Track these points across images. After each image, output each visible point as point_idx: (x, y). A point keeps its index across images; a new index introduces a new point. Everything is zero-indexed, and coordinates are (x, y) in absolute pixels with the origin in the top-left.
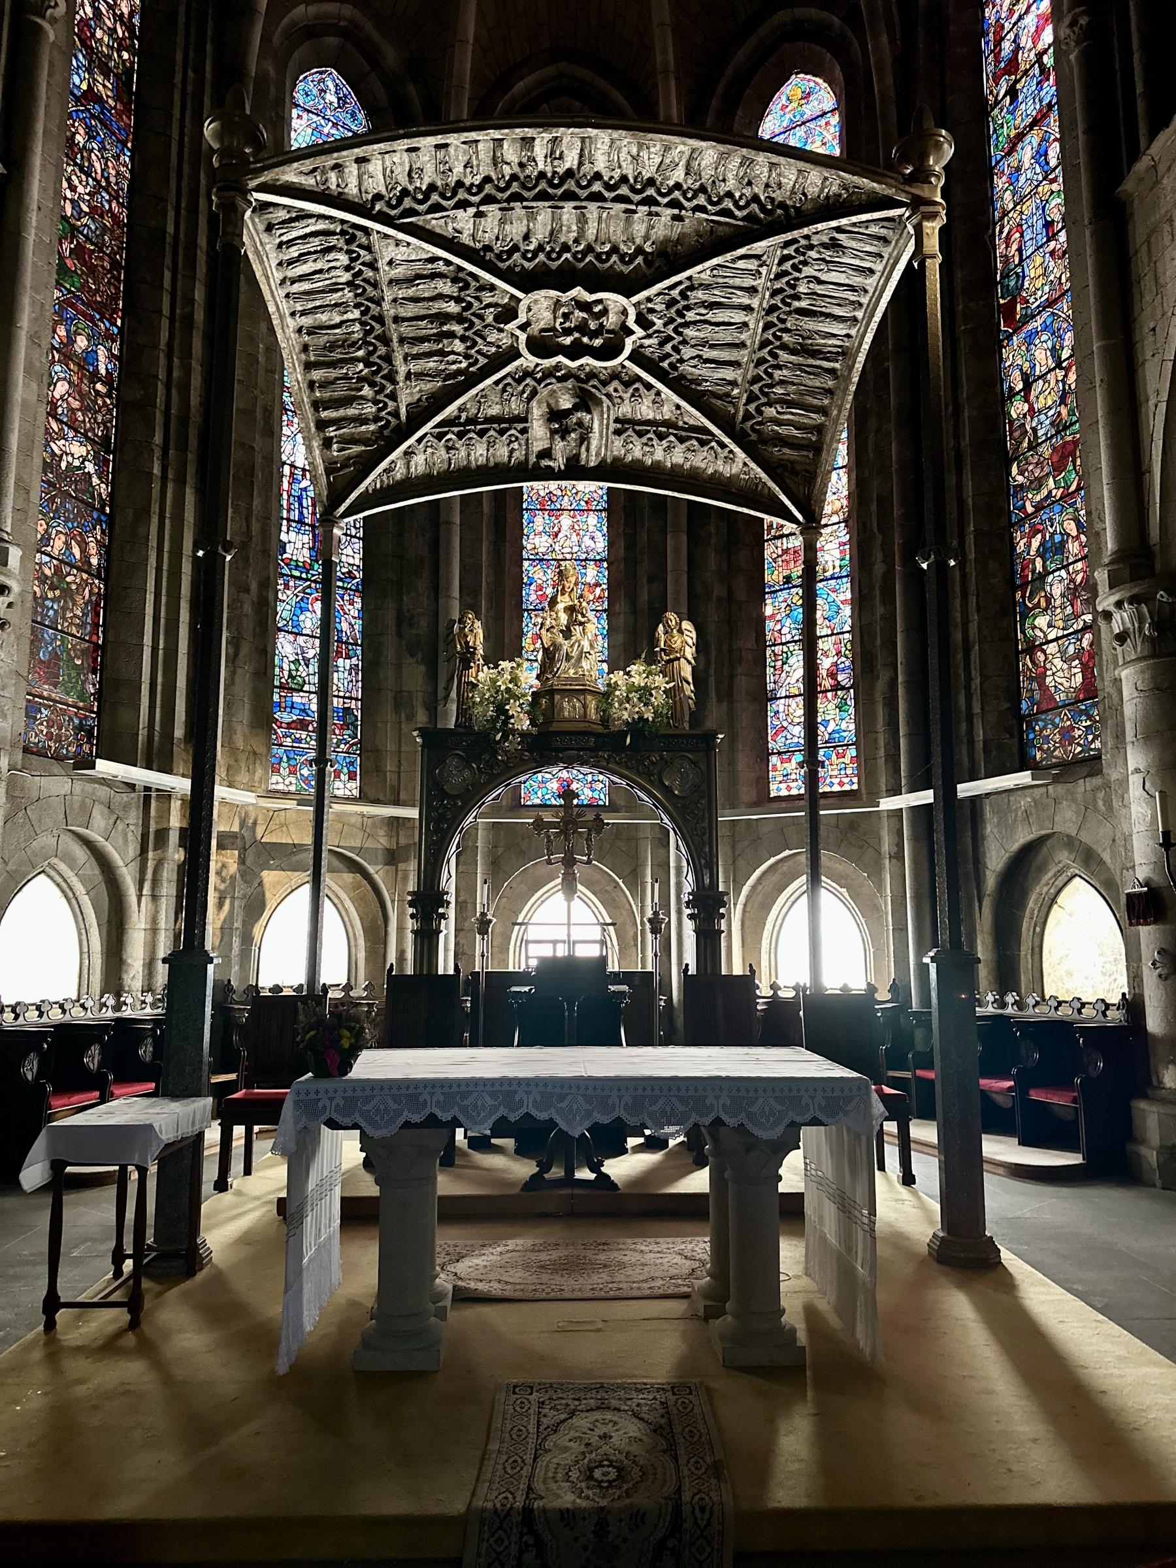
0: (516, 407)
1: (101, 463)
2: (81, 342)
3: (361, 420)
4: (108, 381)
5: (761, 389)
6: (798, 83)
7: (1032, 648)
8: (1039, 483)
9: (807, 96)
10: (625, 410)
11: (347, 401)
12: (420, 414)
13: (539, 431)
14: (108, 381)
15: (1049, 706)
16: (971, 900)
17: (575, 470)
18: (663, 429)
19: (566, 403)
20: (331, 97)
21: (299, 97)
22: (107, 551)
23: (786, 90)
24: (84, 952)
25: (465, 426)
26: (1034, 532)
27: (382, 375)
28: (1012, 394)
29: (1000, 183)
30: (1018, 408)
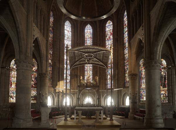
0: (85, 60)
1: (51, 61)
2: (50, 52)
3: (73, 61)
4: (52, 54)
5: (103, 59)
6: (109, 21)
7: (126, 77)
8: (126, 63)
9: (110, 23)
10: (93, 60)
11: (72, 60)
12: (77, 61)
13: (86, 61)
14: (52, 54)
15: (127, 82)
17: (89, 64)
18: (96, 61)
19: (88, 59)
20: (68, 24)
21: (65, 24)
22: (52, 69)
23: (108, 22)
24: (52, 100)
25: (81, 61)
26: (126, 67)
27: (75, 58)
28: (125, 55)
29: (125, 35)
30: (125, 56)
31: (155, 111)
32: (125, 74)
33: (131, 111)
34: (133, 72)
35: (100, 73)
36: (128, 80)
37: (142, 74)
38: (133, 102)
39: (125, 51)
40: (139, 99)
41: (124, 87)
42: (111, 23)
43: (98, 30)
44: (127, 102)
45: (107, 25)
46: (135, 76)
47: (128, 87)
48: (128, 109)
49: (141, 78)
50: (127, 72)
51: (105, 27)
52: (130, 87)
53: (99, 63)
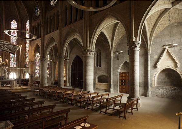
16: (21, 73)
30: (26, 48)
31: (45, 81)
32: (25, 59)
33: (30, 81)
34: (32, 60)
35: (5, 55)
36: (27, 63)
37: (36, 61)
38: (32, 76)
39: (26, 45)
40: (35, 75)
41: (25, 67)
42: (16, 23)
43: (4, 24)
44: (27, 76)
45: (12, 23)
46: (33, 62)
47: (28, 68)
48: (28, 80)
49: (36, 63)
50: (27, 58)
51: (10, 24)
52: (30, 68)
53: (8, 51)
